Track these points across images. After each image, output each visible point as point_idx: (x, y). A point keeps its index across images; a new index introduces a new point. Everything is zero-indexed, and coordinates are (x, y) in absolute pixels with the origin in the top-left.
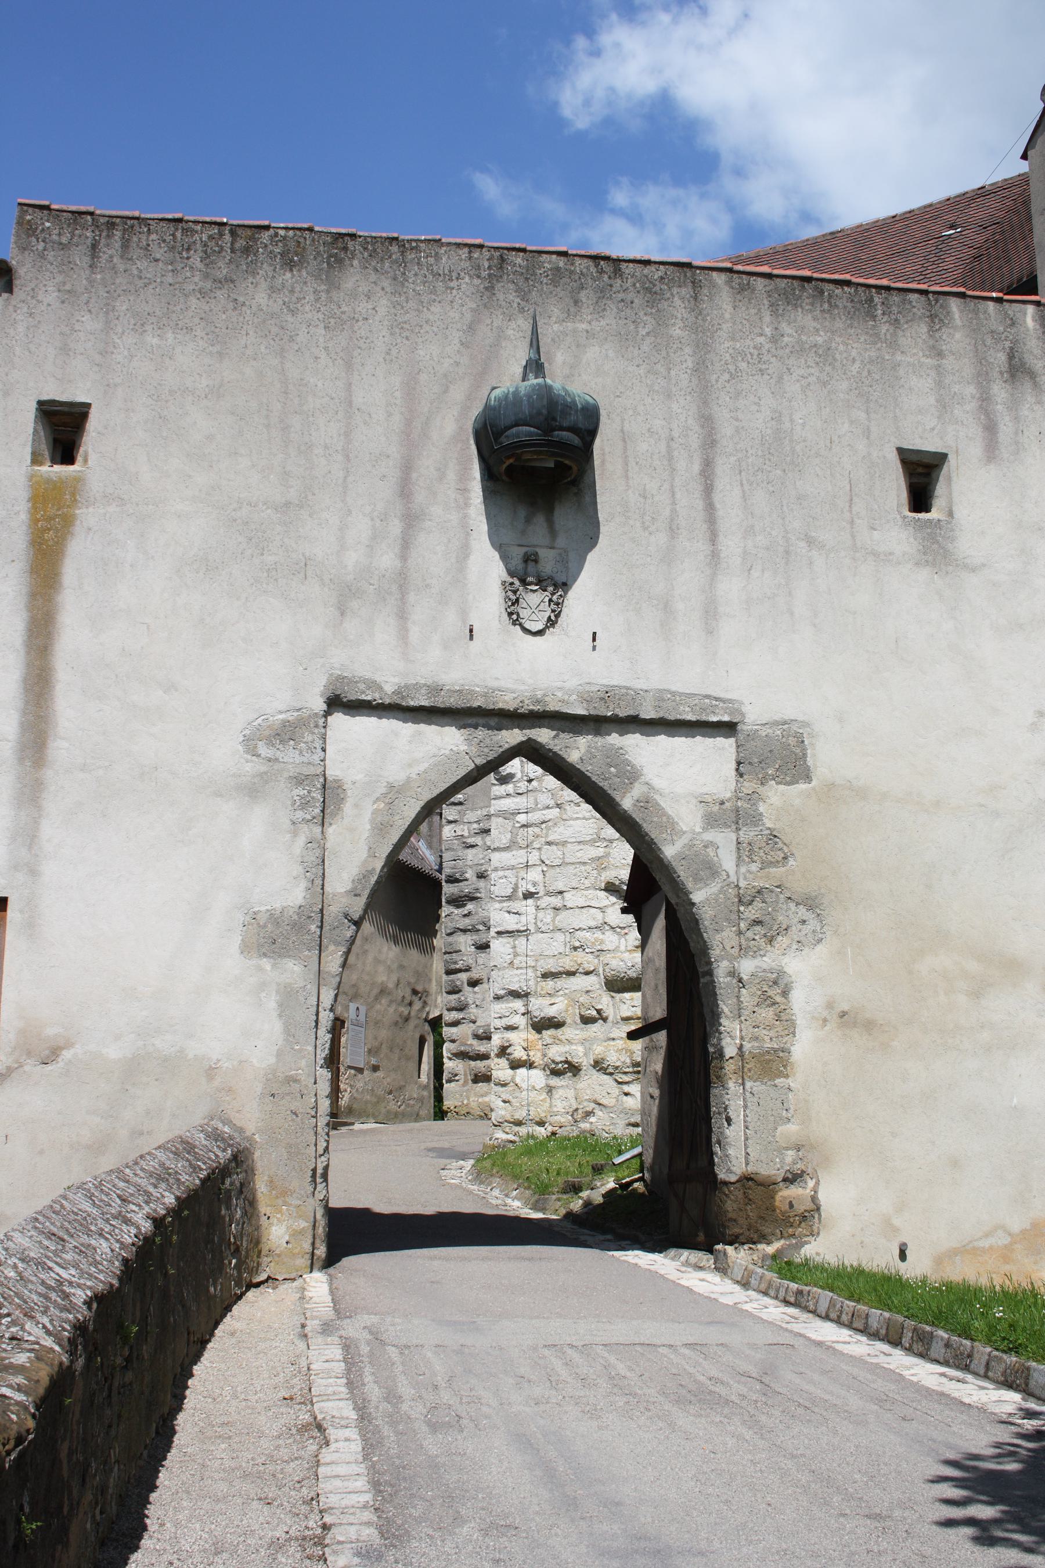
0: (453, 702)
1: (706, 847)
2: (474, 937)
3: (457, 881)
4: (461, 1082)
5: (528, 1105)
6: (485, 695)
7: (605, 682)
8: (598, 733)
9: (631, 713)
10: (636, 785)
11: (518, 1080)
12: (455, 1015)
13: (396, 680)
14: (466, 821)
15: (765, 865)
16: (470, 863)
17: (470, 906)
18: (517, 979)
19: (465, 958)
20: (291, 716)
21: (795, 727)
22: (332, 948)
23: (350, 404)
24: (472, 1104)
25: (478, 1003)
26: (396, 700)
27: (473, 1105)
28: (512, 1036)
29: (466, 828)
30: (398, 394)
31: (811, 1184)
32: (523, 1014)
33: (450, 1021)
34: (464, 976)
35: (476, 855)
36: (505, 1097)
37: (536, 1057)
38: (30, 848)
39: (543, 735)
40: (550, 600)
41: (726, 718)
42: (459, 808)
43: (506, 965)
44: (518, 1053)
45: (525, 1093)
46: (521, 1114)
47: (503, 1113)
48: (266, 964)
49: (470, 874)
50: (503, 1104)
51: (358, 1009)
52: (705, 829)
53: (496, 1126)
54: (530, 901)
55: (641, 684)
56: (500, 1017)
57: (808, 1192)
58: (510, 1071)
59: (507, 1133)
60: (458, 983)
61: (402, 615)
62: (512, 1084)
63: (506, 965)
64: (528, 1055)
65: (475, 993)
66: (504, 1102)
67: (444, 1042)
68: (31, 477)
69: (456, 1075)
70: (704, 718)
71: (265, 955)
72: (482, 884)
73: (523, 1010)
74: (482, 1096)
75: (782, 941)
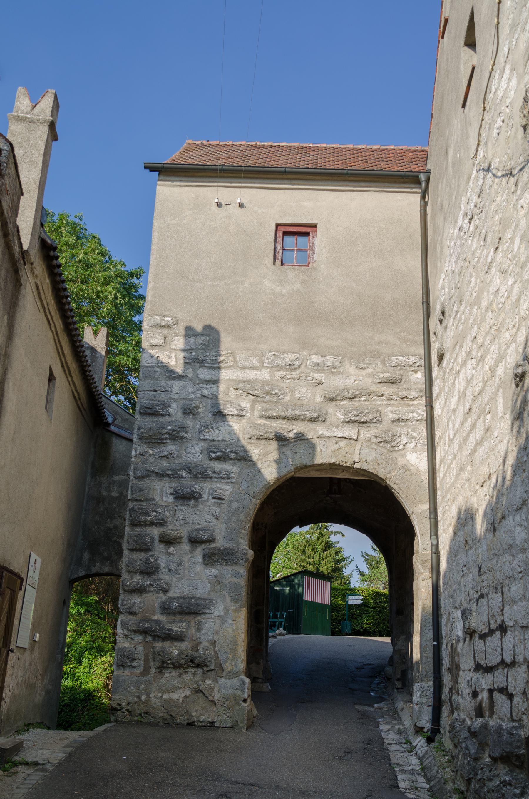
2: (174, 485)
3: (155, 414)
4: (138, 671)
12: (137, 579)
14: (174, 347)
16: (176, 397)
17: (171, 447)
19: (159, 510)
24: (153, 700)
25: (172, 568)
27: (155, 702)
29: (173, 355)
33: (131, 588)
34: (156, 532)
35: (184, 387)
42: (166, 331)
49: (174, 409)
60: (147, 540)
65: (170, 554)
69: (134, 659)
72: (189, 422)
74: (169, 691)
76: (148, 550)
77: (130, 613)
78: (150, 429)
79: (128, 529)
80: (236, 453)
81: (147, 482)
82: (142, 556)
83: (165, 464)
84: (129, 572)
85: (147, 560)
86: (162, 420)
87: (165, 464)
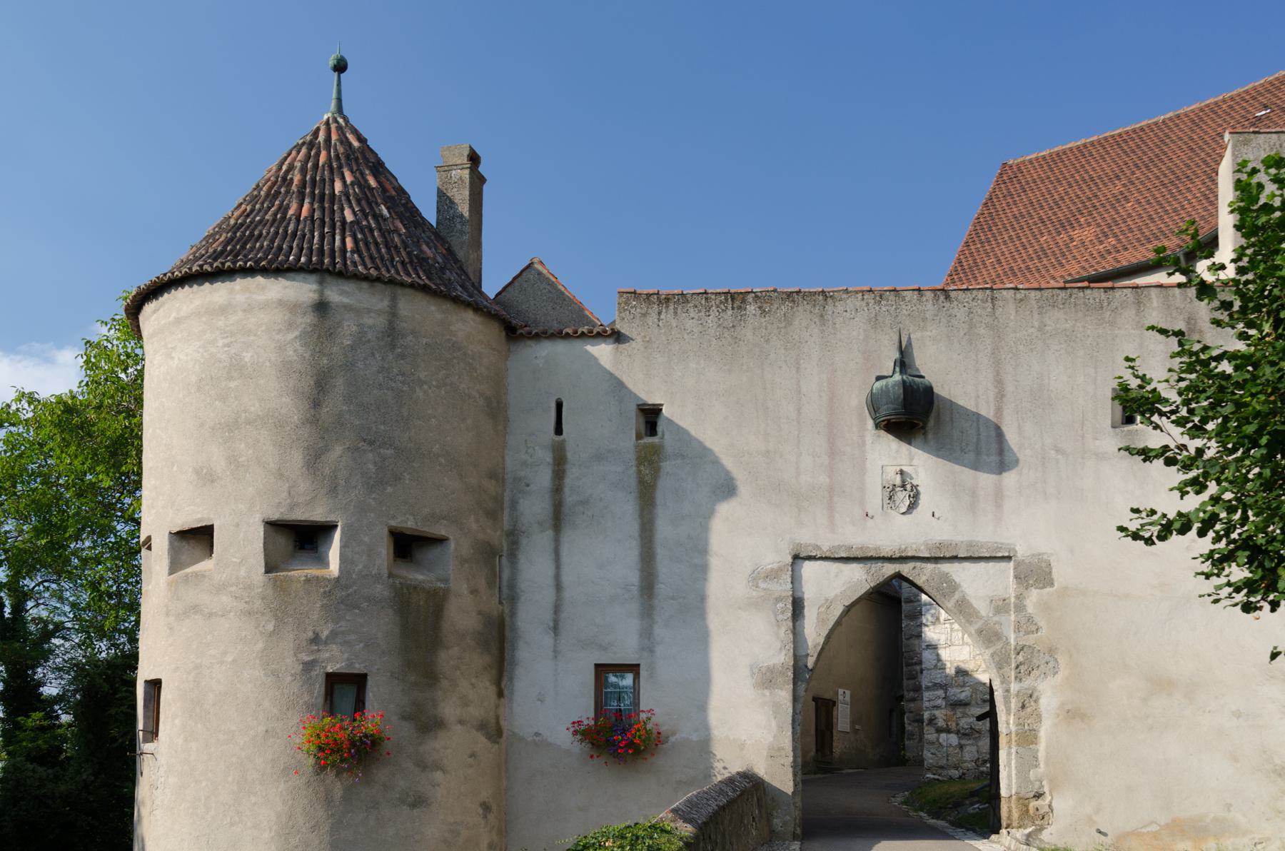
0: (860, 554)
1: (995, 624)
3: (912, 601)
4: (916, 741)
5: (948, 756)
6: (875, 549)
7: (939, 538)
8: (937, 563)
9: (954, 554)
10: (957, 592)
11: (941, 740)
12: (911, 694)
13: (828, 544)
15: (1027, 633)
18: (939, 676)
20: (775, 566)
21: (1045, 557)
22: (799, 683)
23: (799, 392)
26: (828, 554)
28: (937, 713)
30: (825, 384)
31: (1048, 798)
36: (932, 751)
37: (953, 726)
38: (649, 640)
39: (906, 569)
40: (910, 496)
41: (1006, 554)
44: (941, 723)
46: (943, 762)
47: (931, 761)
48: (767, 692)
52: (995, 615)
54: (947, 625)
55: (958, 538)
57: (1047, 802)
58: (936, 735)
59: (934, 774)
61: (831, 509)
64: (947, 725)
66: (932, 754)
67: (904, 713)
68: (636, 447)
70: (994, 555)
71: (766, 688)
73: (943, 695)
75: (1035, 673)
76: (915, 678)
79: (904, 668)
82: (913, 681)
86: (915, 604)
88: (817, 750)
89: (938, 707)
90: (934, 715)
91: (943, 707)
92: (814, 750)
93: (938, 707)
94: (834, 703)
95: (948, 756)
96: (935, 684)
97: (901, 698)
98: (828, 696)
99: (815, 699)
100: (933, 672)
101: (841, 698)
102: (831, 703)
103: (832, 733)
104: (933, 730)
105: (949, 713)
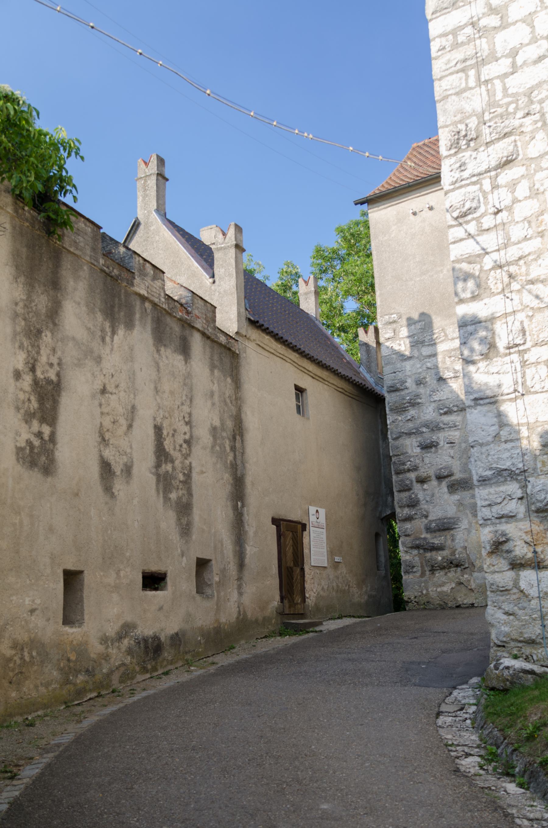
2: (419, 439)
3: (397, 390)
4: (418, 574)
11: (523, 585)
14: (401, 336)
16: (409, 373)
17: (412, 412)
18: (506, 455)
19: (412, 459)
24: (431, 593)
25: (428, 499)
27: (433, 595)
28: (509, 528)
29: (402, 342)
32: (521, 498)
33: (403, 518)
34: (412, 476)
35: (413, 365)
36: (507, 607)
42: (394, 326)
43: (490, 439)
45: (534, 602)
49: (410, 383)
50: (505, 617)
51: (317, 511)
53: (499, 646)
54: (515, 357)
56: (490, 505)
58: (511, 574)
59: (516, 657)
60: (408, 482)
62: (515, 590)
63: (490, 439)
64: (535, 552)
65: (425, 490)
66: (507, 613)
69: (413, 567)
72: (421, 390)
73: (519, 493)
74: (440, 586)
76: (409, 489)
77: (406, 536)
78: (395, 402)
79: (394, 477)
80: (458, 406)
81: (401, 441)
82: (406, 494)
83: (411, 425)
84: (400, 507)
85: (410, 496)
86: (403, 393)
87: (411, 425)
88: (282, 598)
89: (510, 517)
90: (504, 534)
91: (521, 516)
92: (278, 598)
93: (510, 517)
94: (304, 527)
95: (542, 618)
96: (500, 472)
97: (393, 515)
98: (295, 516)
99: (276, 521)
100: (494, 449)
101: (313, 518)
102: (299, 526)
103: (303, 570)
104: (502, 564)
105: (536, 528)
